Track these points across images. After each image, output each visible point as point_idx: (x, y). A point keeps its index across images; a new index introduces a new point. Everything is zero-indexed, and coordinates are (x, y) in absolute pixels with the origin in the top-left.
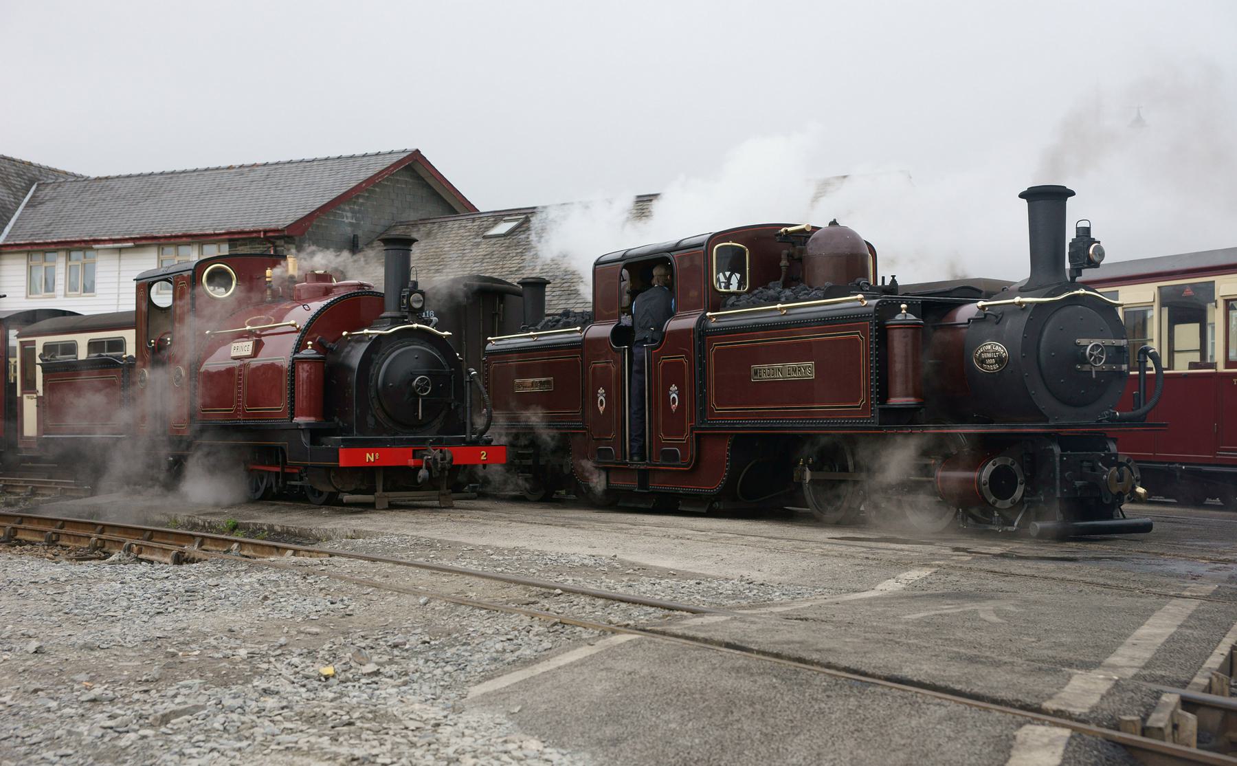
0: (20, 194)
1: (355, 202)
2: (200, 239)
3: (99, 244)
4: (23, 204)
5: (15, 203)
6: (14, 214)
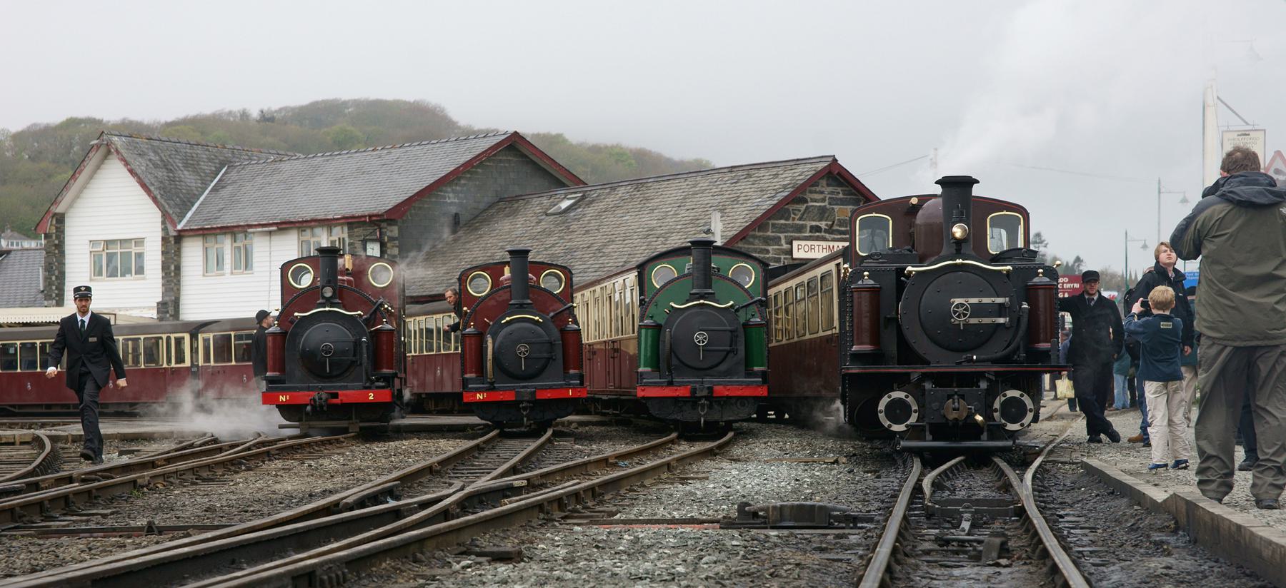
0: (209, 178)
2: (328, 223)
3: (251, 228)
4: (210, 188)
5: (201, 188)
6: (198, 199)
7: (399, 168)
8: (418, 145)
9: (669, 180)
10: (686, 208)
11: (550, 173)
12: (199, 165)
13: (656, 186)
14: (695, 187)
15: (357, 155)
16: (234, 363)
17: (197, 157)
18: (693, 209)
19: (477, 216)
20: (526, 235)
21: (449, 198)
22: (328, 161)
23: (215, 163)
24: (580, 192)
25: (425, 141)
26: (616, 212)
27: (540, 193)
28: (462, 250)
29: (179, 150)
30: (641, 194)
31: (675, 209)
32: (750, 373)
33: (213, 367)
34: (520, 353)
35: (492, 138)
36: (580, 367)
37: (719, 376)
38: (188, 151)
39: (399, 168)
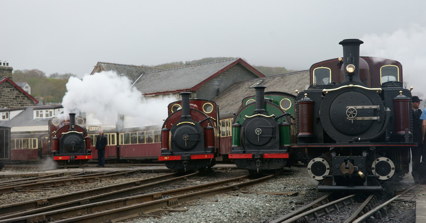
0: (136, 78)
1: (218, 78)
3: (147, 95)
4: (136, 82)
7: (199, 73)
8: (206, 64)
9: (294, 74)
10: (299, 84)
11: (252, 73)
12: (132, 73)
13: (289, 76)
14: (303, 76)
15: (186, 68)
16: (130, 144)
17: (132, 71)
18: (301, 84)
19: (226, 89)
20: (242, 96)
21: (216, 83)
22: (175, 71)
23: (138, 73)
24: (262, 80)
25: (205, 63)
26: (273, 87)
27: (248, 81)
28: (219, 102)
29: (125, 68)
30: (283, 80)
31: (295, 85)
32: (281, 147)
33: (124, 145)
34: (185, 139)
35: (232, 61)
36: (213, 145)
37: (267, 149)
38: (129, 68)
39: (199, 73)
